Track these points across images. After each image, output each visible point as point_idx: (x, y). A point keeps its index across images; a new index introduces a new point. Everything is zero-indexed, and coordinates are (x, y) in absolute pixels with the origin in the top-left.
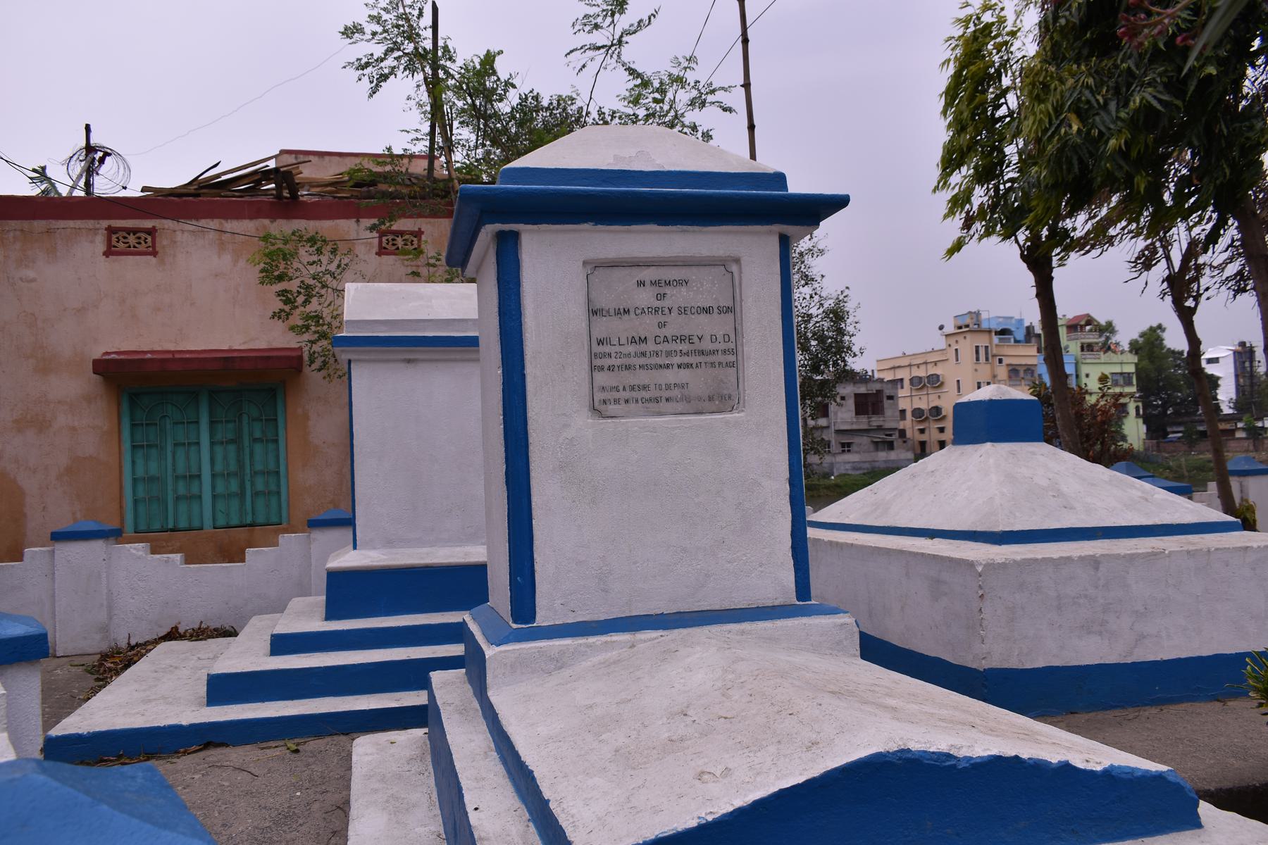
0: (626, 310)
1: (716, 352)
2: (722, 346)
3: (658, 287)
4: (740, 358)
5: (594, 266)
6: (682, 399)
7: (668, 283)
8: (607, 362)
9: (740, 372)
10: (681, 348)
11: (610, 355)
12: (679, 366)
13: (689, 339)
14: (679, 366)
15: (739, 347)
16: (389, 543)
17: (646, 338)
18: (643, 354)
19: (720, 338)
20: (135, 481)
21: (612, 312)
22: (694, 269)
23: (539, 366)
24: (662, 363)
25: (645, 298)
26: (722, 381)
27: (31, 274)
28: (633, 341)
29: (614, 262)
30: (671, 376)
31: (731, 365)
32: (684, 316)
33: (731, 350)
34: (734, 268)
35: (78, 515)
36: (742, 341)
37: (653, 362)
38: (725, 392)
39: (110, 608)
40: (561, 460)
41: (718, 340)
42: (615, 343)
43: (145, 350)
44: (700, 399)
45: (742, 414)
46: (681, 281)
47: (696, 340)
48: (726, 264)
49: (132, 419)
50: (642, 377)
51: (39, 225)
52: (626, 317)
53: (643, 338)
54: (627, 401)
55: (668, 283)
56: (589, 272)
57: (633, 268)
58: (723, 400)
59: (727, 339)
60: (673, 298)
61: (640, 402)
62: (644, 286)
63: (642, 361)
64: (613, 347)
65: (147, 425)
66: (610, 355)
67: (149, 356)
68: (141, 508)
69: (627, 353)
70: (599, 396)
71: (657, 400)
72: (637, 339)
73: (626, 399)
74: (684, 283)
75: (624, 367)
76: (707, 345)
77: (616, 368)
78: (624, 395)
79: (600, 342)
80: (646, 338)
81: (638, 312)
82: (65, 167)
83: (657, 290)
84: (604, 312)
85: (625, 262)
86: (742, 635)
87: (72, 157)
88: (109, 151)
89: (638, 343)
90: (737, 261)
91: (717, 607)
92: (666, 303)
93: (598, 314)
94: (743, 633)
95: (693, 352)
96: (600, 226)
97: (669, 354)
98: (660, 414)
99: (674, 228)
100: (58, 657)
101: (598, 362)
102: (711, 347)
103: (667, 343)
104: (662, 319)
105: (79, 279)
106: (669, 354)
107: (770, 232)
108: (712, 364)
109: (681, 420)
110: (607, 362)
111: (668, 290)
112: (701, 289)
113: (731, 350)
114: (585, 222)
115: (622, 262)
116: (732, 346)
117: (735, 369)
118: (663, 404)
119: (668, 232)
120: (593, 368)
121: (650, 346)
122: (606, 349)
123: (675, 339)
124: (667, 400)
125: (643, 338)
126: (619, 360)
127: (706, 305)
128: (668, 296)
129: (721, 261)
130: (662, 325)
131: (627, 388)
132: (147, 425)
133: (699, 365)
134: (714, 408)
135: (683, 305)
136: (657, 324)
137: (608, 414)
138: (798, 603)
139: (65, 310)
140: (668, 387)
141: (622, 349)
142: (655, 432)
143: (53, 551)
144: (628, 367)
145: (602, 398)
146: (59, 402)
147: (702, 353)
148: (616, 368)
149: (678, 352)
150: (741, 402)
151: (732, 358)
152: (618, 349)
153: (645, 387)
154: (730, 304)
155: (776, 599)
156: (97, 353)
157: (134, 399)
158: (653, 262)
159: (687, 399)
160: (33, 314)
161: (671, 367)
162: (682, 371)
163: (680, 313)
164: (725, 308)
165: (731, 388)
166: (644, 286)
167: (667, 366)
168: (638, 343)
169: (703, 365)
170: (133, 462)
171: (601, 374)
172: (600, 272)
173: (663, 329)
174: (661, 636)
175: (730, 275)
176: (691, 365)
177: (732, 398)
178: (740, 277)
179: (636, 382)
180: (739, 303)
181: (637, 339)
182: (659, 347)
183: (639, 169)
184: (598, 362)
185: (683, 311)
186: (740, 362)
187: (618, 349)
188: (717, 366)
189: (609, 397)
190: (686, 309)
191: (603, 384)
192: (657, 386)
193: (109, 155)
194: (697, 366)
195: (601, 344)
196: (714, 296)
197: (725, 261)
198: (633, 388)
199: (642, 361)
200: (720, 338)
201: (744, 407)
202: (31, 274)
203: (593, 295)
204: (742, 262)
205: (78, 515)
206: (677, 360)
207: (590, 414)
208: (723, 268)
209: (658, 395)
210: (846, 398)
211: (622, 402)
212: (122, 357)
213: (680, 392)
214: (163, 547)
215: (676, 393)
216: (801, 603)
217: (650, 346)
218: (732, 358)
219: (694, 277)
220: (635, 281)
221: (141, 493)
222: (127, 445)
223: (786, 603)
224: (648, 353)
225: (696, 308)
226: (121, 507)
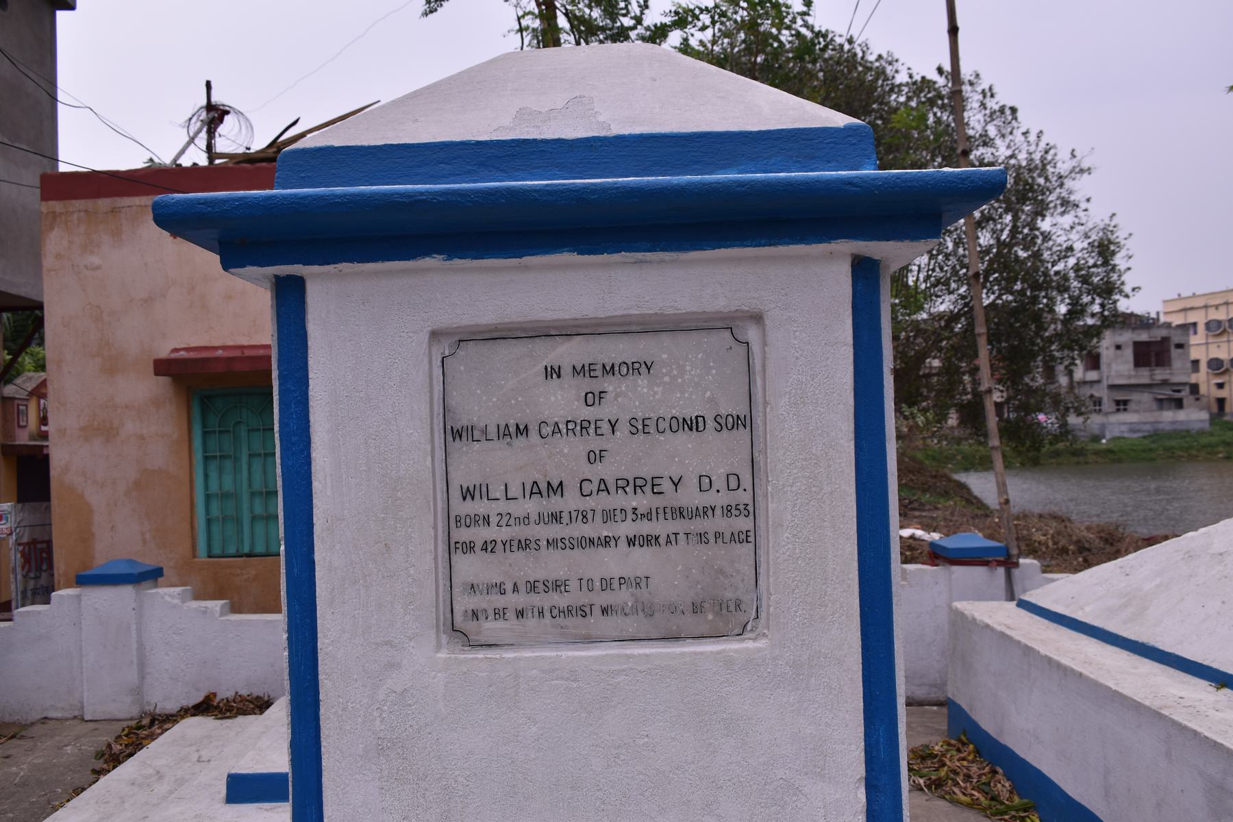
0: (522, 427)
1: (710, 513)
2: (721, 499)
3: (587, 379)
4: (761, 522)
5: (457, 338)
6: (635, 610)
7: (609, 370)
8: (481, 534)
9: (761, 552)
10: (634, 504)
11: (487, 520)
12: (631, 542)
14: (631, 542)
15: (759, 499)
17: (561, 483)
18: (556, 517)
19: (719, 483)
20: (208, 497)
21: (492, 431)
22: (666, 339)
23: (338, 547)
24: (594, 535)
26: (721, 571)
27: (96, 260)
28: (535, 490)
29: (496, 329)
30: (612, 562)
31: (742, 538)
32: (642, 436)
33: (742, 507)
34: (752, 334)
35: (148, 536)
36: (767, 489)
37: (577, 534)
38: (729, 595)
39: (142, 665)
40: (382, 735)
41: (715, 488)
42: (498, 495)
43: (216, 345)
44: (673, 609)
45: (761, 643)
46: (636, 366)
47: (666, 486)
49: (204, 426)
50: (553, 565)
51: (104, 204)
52: (521, 441)
53: (555, 484)
54: (520, 614)
55: (609, 370)
56: (447, 353)
57: (537, 340)
58: (724, 611)
59: (733, 484)
60: (620, 399)
61: (547, 614)
62: (559, 376)
63: (555, 531)
64: (494, 504)
65: (220, 432)
66: (487, 520)
67: (220, 353)
68: (216, 529)
69: (522, 514)
70: (464, 603)
71: (583, 612)
72: (543, 486)
73: (520, 608)
74: (643, 369)
75: (515, 543)
76: (690, 497)
77: (500, 546)
78: (513, 601)
79: (468, 494)
80: (561, 483)
81: (547, 430)
82: (186, 130)
83: (586, 384)
84: (475, 433)
85: (517, 329)
87: (190, 119)
88: (228, 109)
89: (545, 493)
90: (757, 318)
92: (605, 411)
93: (464, 438)
95: (661, 511)
96: (458, 262)
97: (609, 516)
98: (590, 640)
99: (616, 257)
100: (87, 721)
101: (463, 535)
102: (700, 500)
103: (605, 493)
104: (595, 444)
105: (146, 264)
106: (609, 516)
108: (702, 537)
109: (629, 657)
110: (481, 534)
111: (609, 385)
112: (680, 380)
113: (742, 507)
114: (427, 253)
115: (510, 330)
116: (745, 497)
117: (751, 546)
118: (597, 623)
119: (607, 265)
120: (453, 547)
121: (571, 501)
122: (479, 507)
123: (623, 485)
124: (605, 611)
125: (555, 484)
126: (504, 529)
127: (689, 413)
128: (608, 397)
129: (723, 319)
130: (595, 457)
131: (522, 588)
132: (220, 432)
133: (673, 537)
134: (704, 629)
135: (640, 415)
136: (585, 454)
137: (483, 640)
139: (131, 301)
140: (607, 584)
141: (512, 507)
142: (575, 681)
143: (79, 597)
144: (524, 545)
145: (472, 607)
146: (127, 407)
147: (680, 513)
148: (500, 546)
150: (763, 615)
151: (743, 524)
152: (503, 506)
153: (558, 586)
154: (742, 410)
156: (164, 352)
157: (206, 403)
159: (648, 611)
160: (98, 307)
161: (613, 543)
162: (637, 551)
163: (634, 430)
164: (730, 419)
165: (741, 585)
166: (559, 376)
167: (606, 542)
168: (545, 493)
169: (681, 537)
170: (206, 476)
171: (470, 557)
172: (471, 349)
173: (599, 466)
175: (741, 349)
176: (657, 539)
177: (743, 607)
178: (764, 358)
179: (540, 575)
180: (761, 408)
181: (543, 486)
182: (590, 503)
183: (556, 137)
184: (463, 535)
185: (640, 427)
186: (761, 532)
187: (503, 506)
188: (712, 540)
189: (484, 606)
190: (647, 422)
191: (471, 579)
192: (584, 583)
193: (227, 113)
194: (668, 542)
195: (469, 497)
196: (708, 394)
197: (733, 319)
198: (533, 587)
199: (555, 531)
200: (719, 483)
201: (768, 628)
202: (96, 260)
203: (452, 402)
204: (767, 322)
205: (148, 536)
206: (626, 528)
207: (444, 639)
208: (727, 334)
209: (587, 601)
210: (1123, 347)
211: (511, 614)
212: (192, 355)
213: (633, 595)
214: (238, 575)
215: (623, 596)
217: (571, 501)
218: (743, 524)
219: (665, 356)
220: (541, 367)
221: (215, 512)
222: (198, 456)
224: (565, 516)
225: (668, 420)
226: (192, 527)
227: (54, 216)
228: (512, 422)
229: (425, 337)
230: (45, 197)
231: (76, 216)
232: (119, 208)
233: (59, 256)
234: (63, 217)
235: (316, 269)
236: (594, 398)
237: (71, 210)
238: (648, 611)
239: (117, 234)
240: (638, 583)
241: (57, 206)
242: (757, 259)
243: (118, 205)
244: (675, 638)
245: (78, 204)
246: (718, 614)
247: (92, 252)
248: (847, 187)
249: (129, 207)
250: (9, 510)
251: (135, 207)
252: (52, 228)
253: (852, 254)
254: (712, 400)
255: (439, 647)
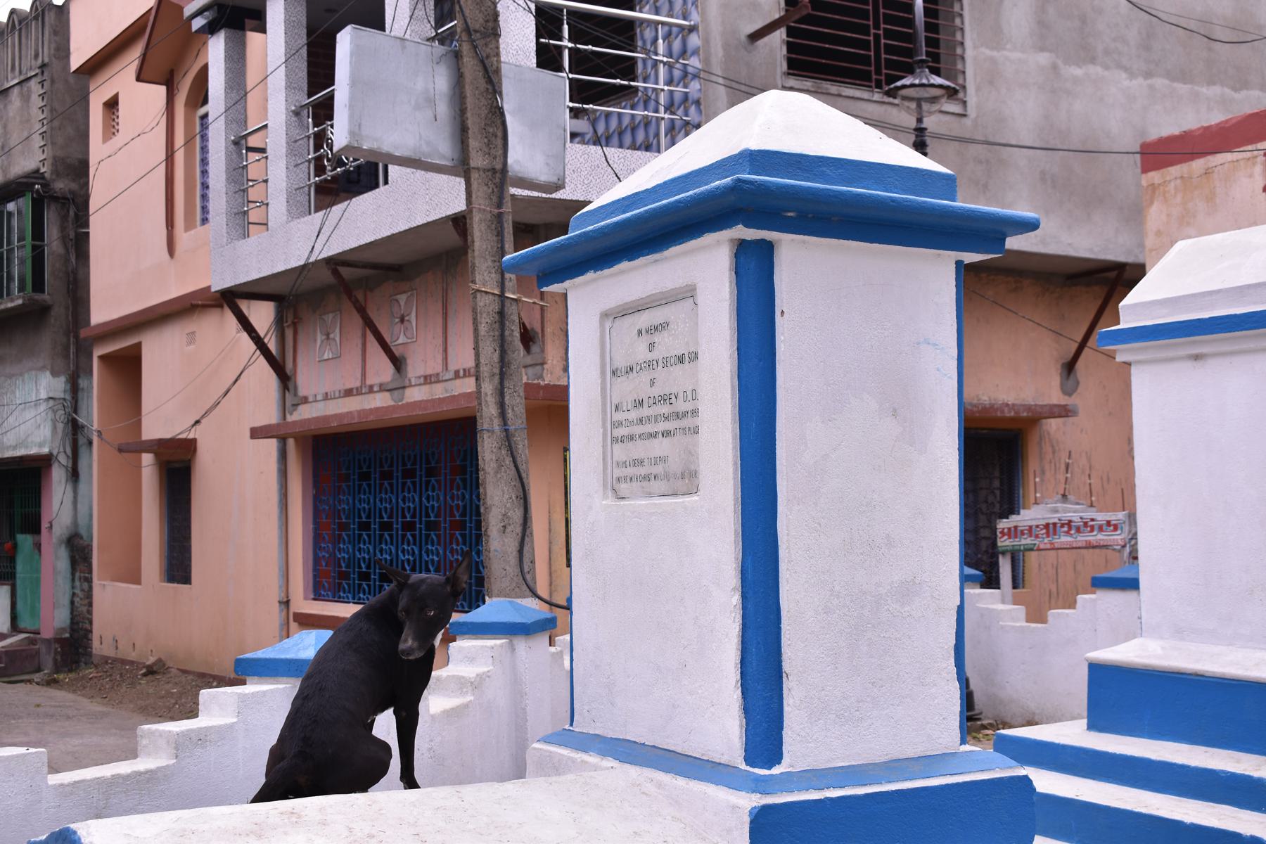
2: (688, 406)
7: (656, 329)
13: (666, 399)
16: (1179, 632)
25: (641, 352)
26: (690, 453)
29: (624, 310)
30: (660, 447)
33: (696, 411)
38: (693, 467)
48: (688, 294)
70: (618, 472)
76: (681, 406)
78: (630, 471)
79: (617, 409)
86: (659, 789)
91: (679, 750)
92: (656, 355)
94: (660, 785)
97: (656, 419)
98: (650, 495)
106: (656, 419)
107: (718, 243)
109: (655, 504)
111: (657, 338)
118: (656, 486)
122: (619, 416)
127: (679, 353)
129: (686, 292)
138: (743, 767)
144: (632, 438)
147: (677, 416)
149: (662, 415)
155: (723, 754)
158: (646, 304)
159: (667, 477)
162: (666, 441)
167: (654, 435)
174: (612, 767)
183: (645, 188)
185: (666, 363)
207: (610, 493)
209: (649, 472)
216: (748, 768)
217: (645, 411)
223: (729, 764)
227: (1153, 187)
228: (629, 364)
229: (597, 318)
230: (1145, 169)
231: (1172, 184)
232: (1212, 167)
233: (1159, 233)
234: (1161, 188)
235: (567, 284)
236: (652, 346)
237: (1168, 178)
238: (667, 477)
239: (1210, 198)
240: (663, 459)
241: (1155, 176)
242: (692, 251)
243: (1211, 165)
244: (675, 495)
245: (1174, 171)
246: (689, 480)
247: (1188, 224)
248: (679, 204)
249: (1221, 165)
250: (1124, 519)
251: (1226, 165)
252: (1152, 203)
253: (732, 240)
254: (687, 343)
255: (605, 497)
